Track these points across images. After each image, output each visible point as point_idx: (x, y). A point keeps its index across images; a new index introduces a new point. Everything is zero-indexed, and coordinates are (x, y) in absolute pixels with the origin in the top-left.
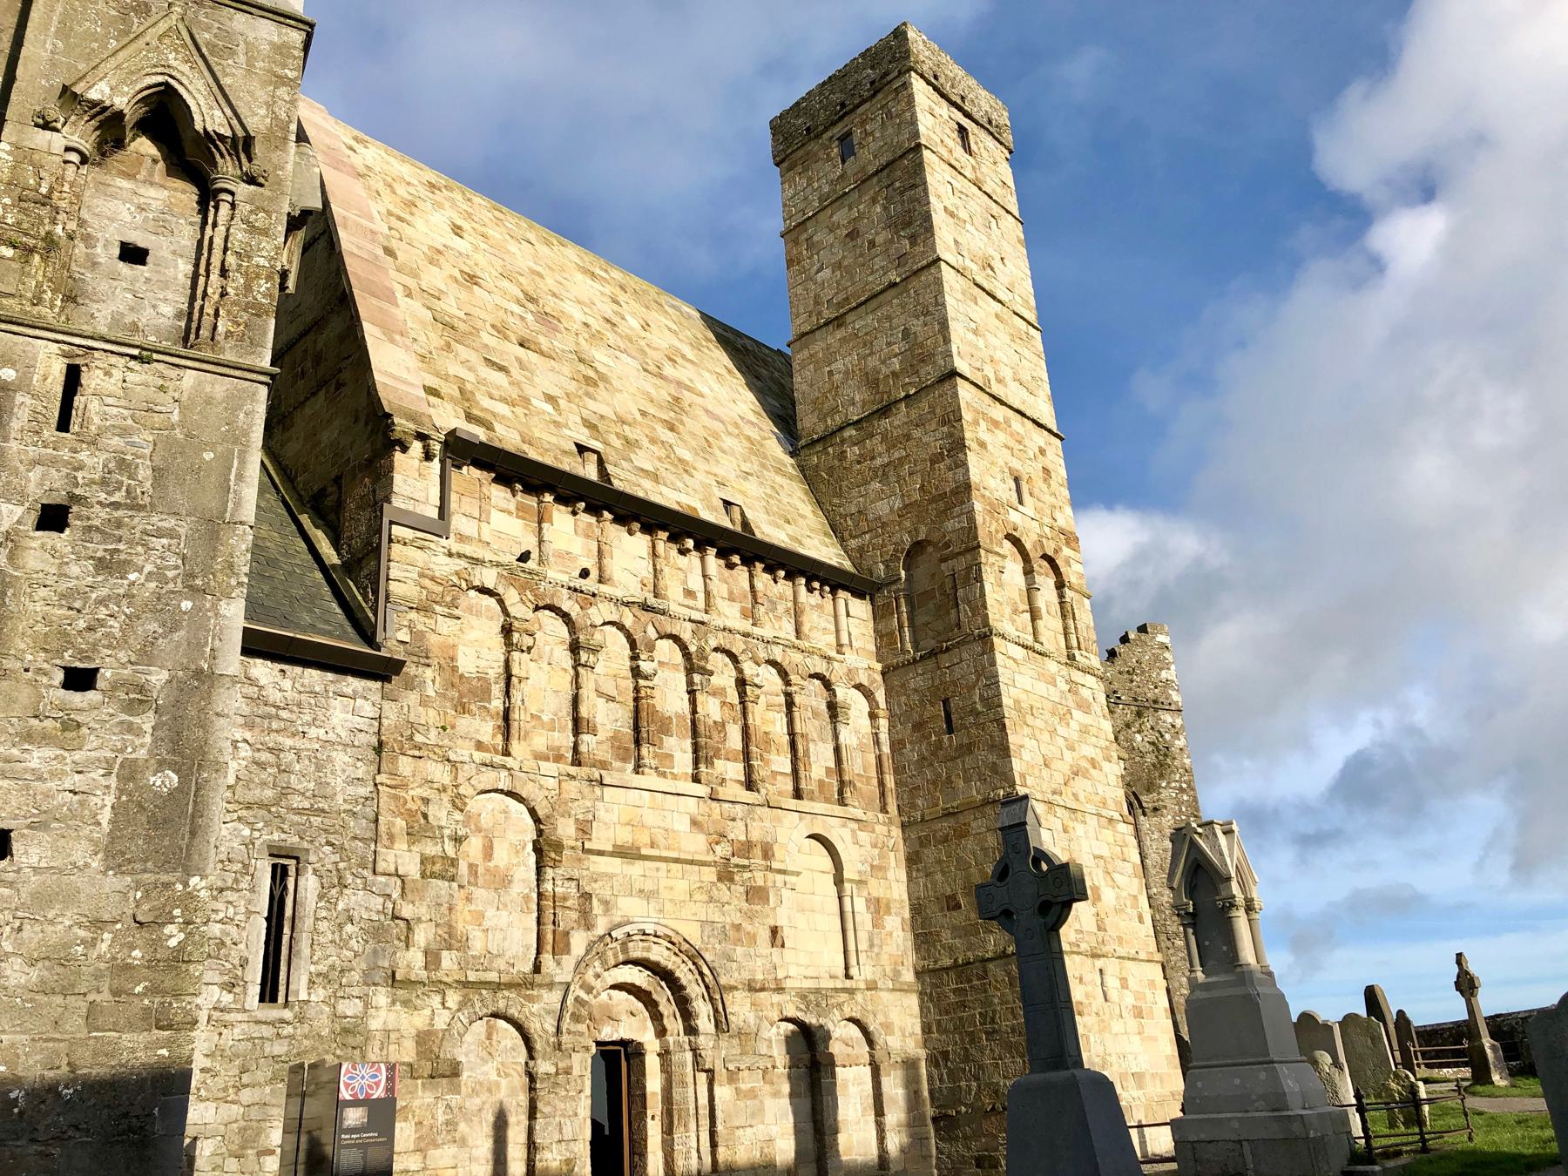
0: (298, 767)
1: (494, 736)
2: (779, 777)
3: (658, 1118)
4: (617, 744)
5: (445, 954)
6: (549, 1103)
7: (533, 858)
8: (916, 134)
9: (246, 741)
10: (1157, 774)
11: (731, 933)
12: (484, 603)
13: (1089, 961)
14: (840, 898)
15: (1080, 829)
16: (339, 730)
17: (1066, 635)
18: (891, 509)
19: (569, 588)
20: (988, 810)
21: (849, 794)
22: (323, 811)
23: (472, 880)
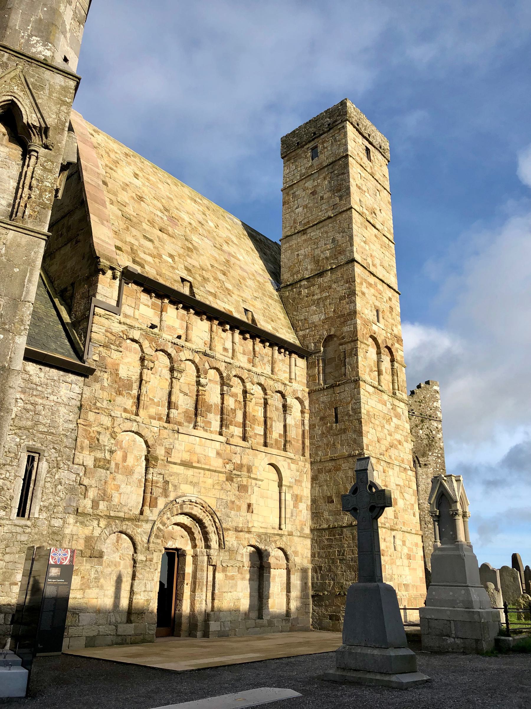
0: (43, 413)
1: (132, 406)
2: (257, 436)
3: (189, 585)
4: (187, 415)
5: (101, 502)
6: (141, 574)
7: (144, 463)
8: (347, 150)
9: (21, 399)
10: (428, 449)
11: (230, 504)
12: (133, 346)
13: (389, 532)
14: (280, 493)
15: (391, 472)
16: (63, 398)
17: (393, 383)
18: (320, 320)
19: (172, 343)
20: (350, 459)
21: (288, 447)
22: (53, 433)
23: (116, 470)
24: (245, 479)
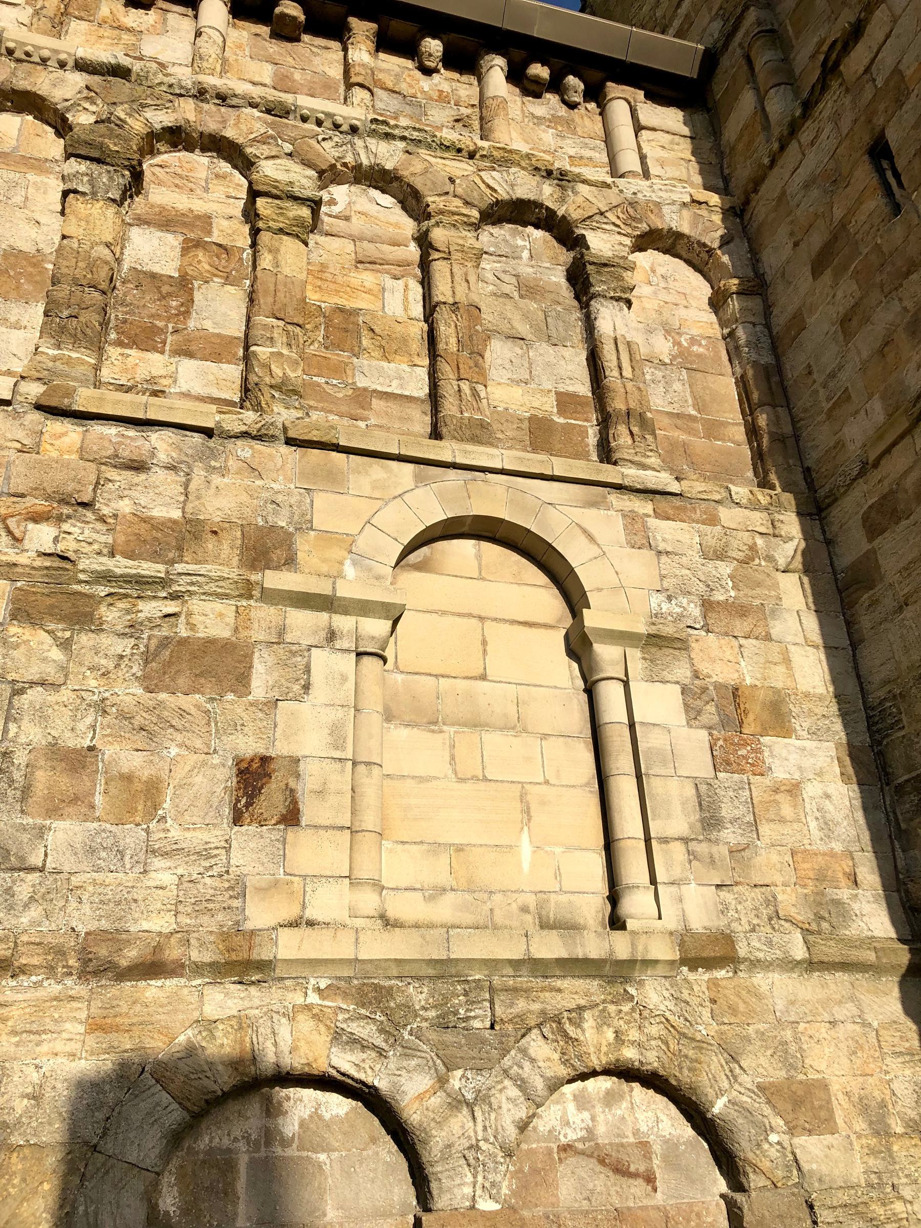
2: (376, 403)
14: (590, 691)
24: (227, 608)
